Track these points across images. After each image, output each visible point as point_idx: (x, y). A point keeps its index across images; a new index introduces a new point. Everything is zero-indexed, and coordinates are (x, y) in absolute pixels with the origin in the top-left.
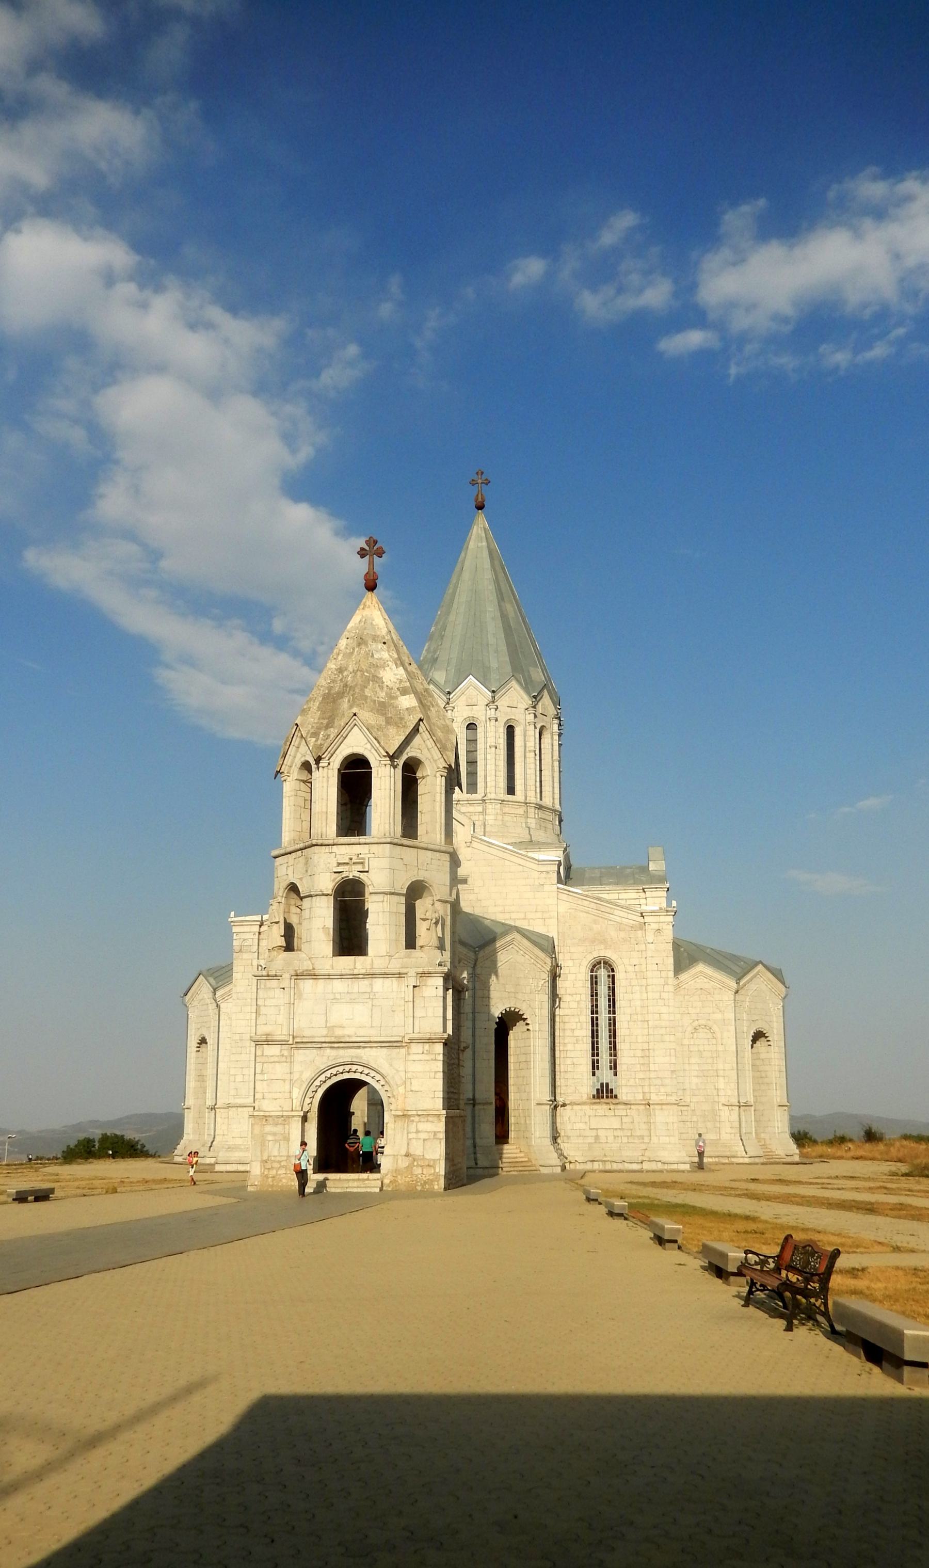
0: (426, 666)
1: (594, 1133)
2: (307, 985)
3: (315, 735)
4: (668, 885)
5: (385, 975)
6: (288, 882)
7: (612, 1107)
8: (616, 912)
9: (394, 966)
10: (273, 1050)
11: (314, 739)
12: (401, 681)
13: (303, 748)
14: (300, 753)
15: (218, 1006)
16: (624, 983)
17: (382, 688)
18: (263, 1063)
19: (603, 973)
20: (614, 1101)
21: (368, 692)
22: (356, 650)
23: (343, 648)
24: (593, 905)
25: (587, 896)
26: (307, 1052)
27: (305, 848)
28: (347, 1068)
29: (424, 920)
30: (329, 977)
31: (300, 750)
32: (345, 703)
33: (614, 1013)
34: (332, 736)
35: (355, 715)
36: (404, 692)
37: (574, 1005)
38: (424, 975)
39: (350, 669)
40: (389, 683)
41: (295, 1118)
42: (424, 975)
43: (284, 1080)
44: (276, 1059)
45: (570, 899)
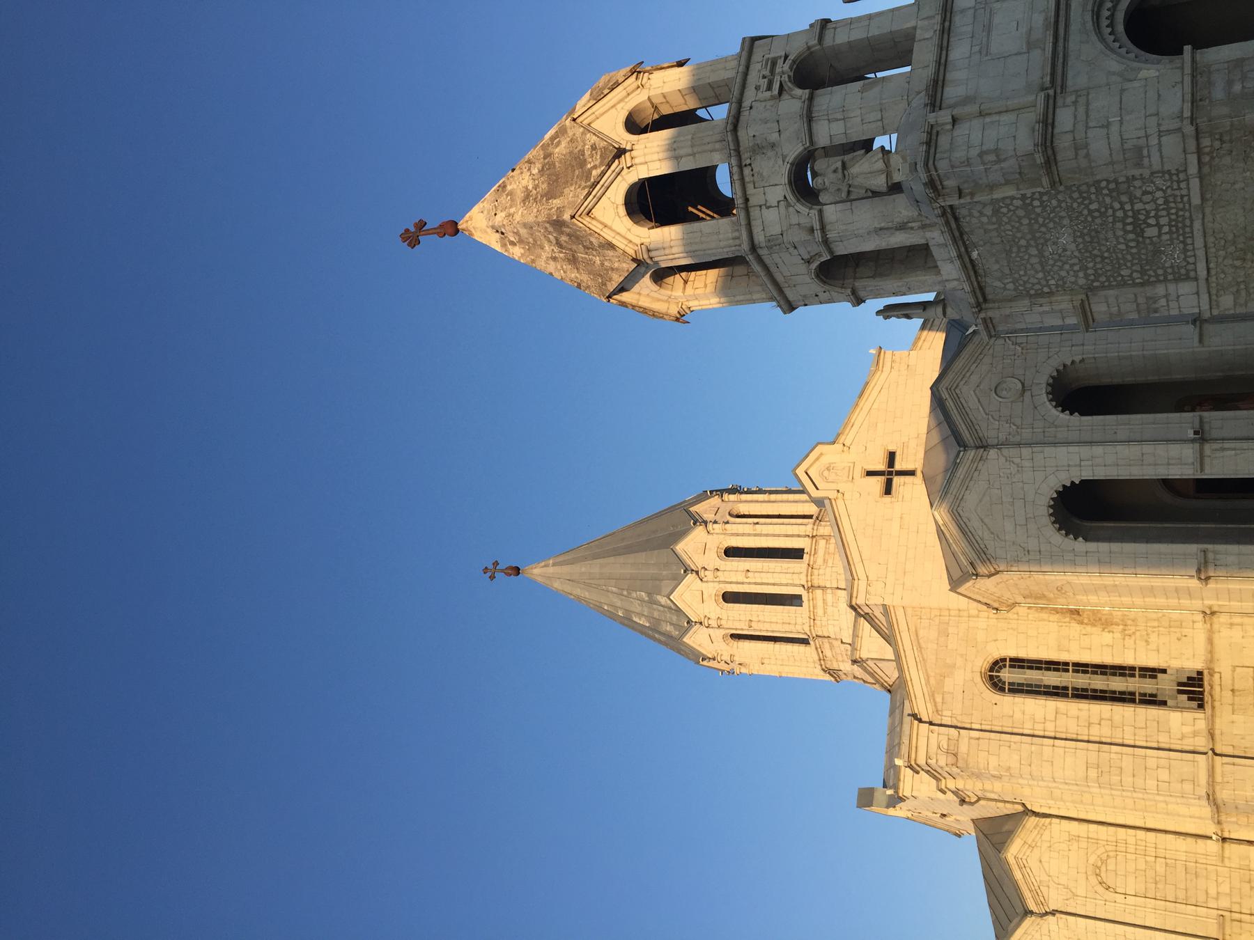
0: (656, 614)
2: (952, 92)
6: (790, 197)
10: (1064, 119)
11: (595, 173)
15: (1053, 913)
18: (1087, 127)
23: (503, 214)
26: (1070, 74)
28: (1105, 22)
30: (942, 64)
31: (609, 224)
35: (574, 120)
41: (1198, 57)
43: (1122, 91)
44: (1081, 110)
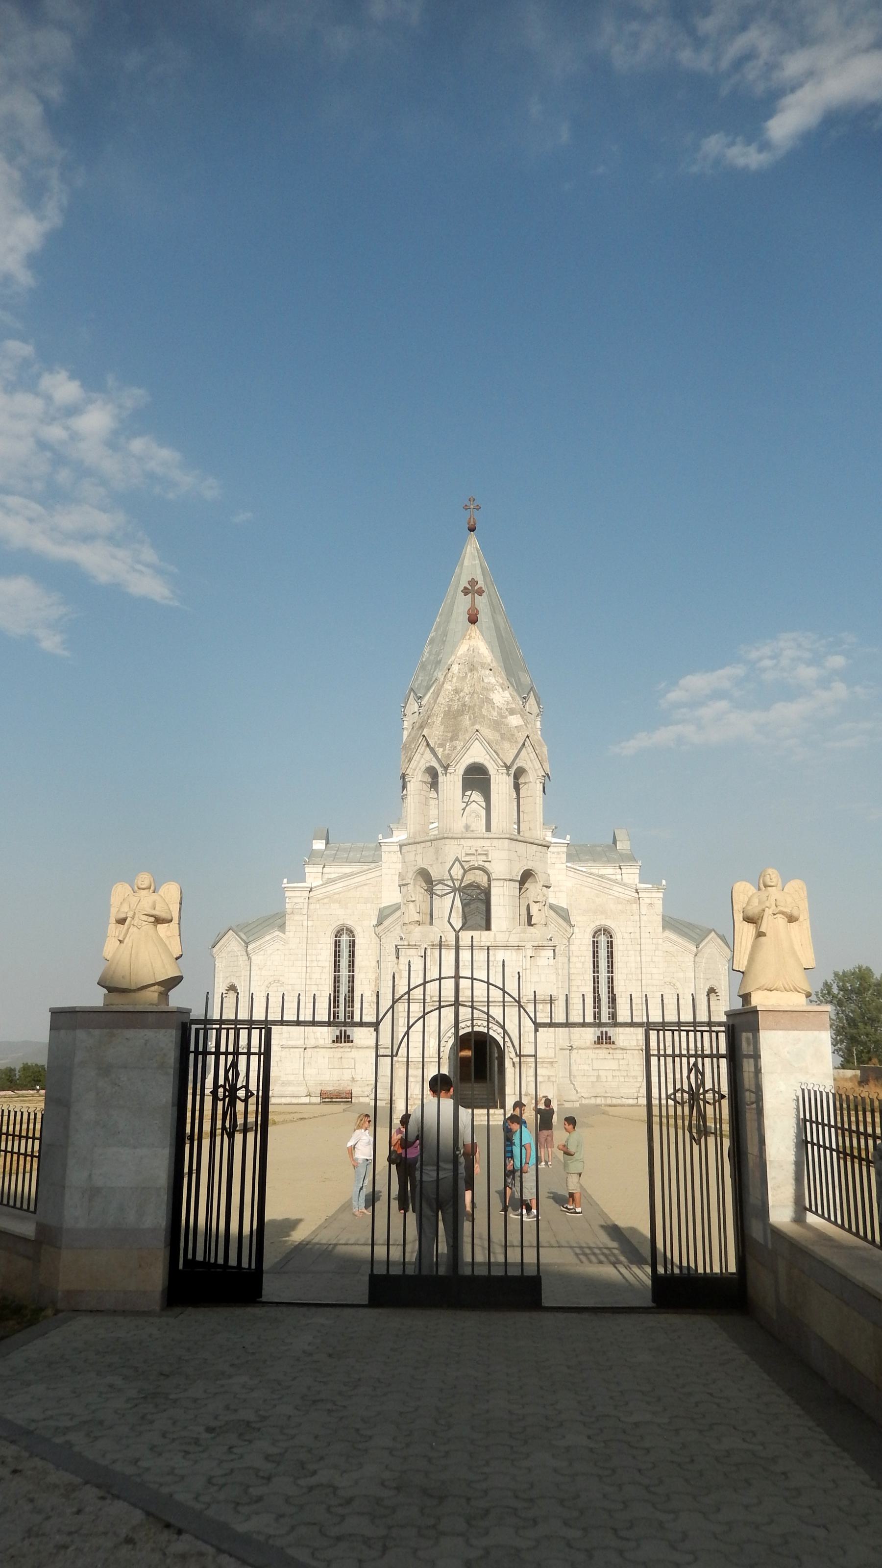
1: (596, 1073)
3: (442, 745)
4: (640, 863)
5: (506, 947)
7: (611, 1051)
8: (615, 888)
9: (514, 940)
12: (508, 703)
13: (428, 755)
14: (423, 759)
16: (621, 948)
17: (494, 708)
19: (603, 940)
20: (613, 1046)
21: (484, 712)
22: (469, 674)
23: (456, 672)
24: (595, 882)
25: (591, 874)
27: (436, 840)
29: (536, 902)
32: (466, 720)
33: (612, 972)
34: (459, 748)
36: (512, 712)
37: (579, 965)
38: (538, 948)
39: (466, 690)
40: (498, 704)
42: (538, 948)
45: (576, 876)
